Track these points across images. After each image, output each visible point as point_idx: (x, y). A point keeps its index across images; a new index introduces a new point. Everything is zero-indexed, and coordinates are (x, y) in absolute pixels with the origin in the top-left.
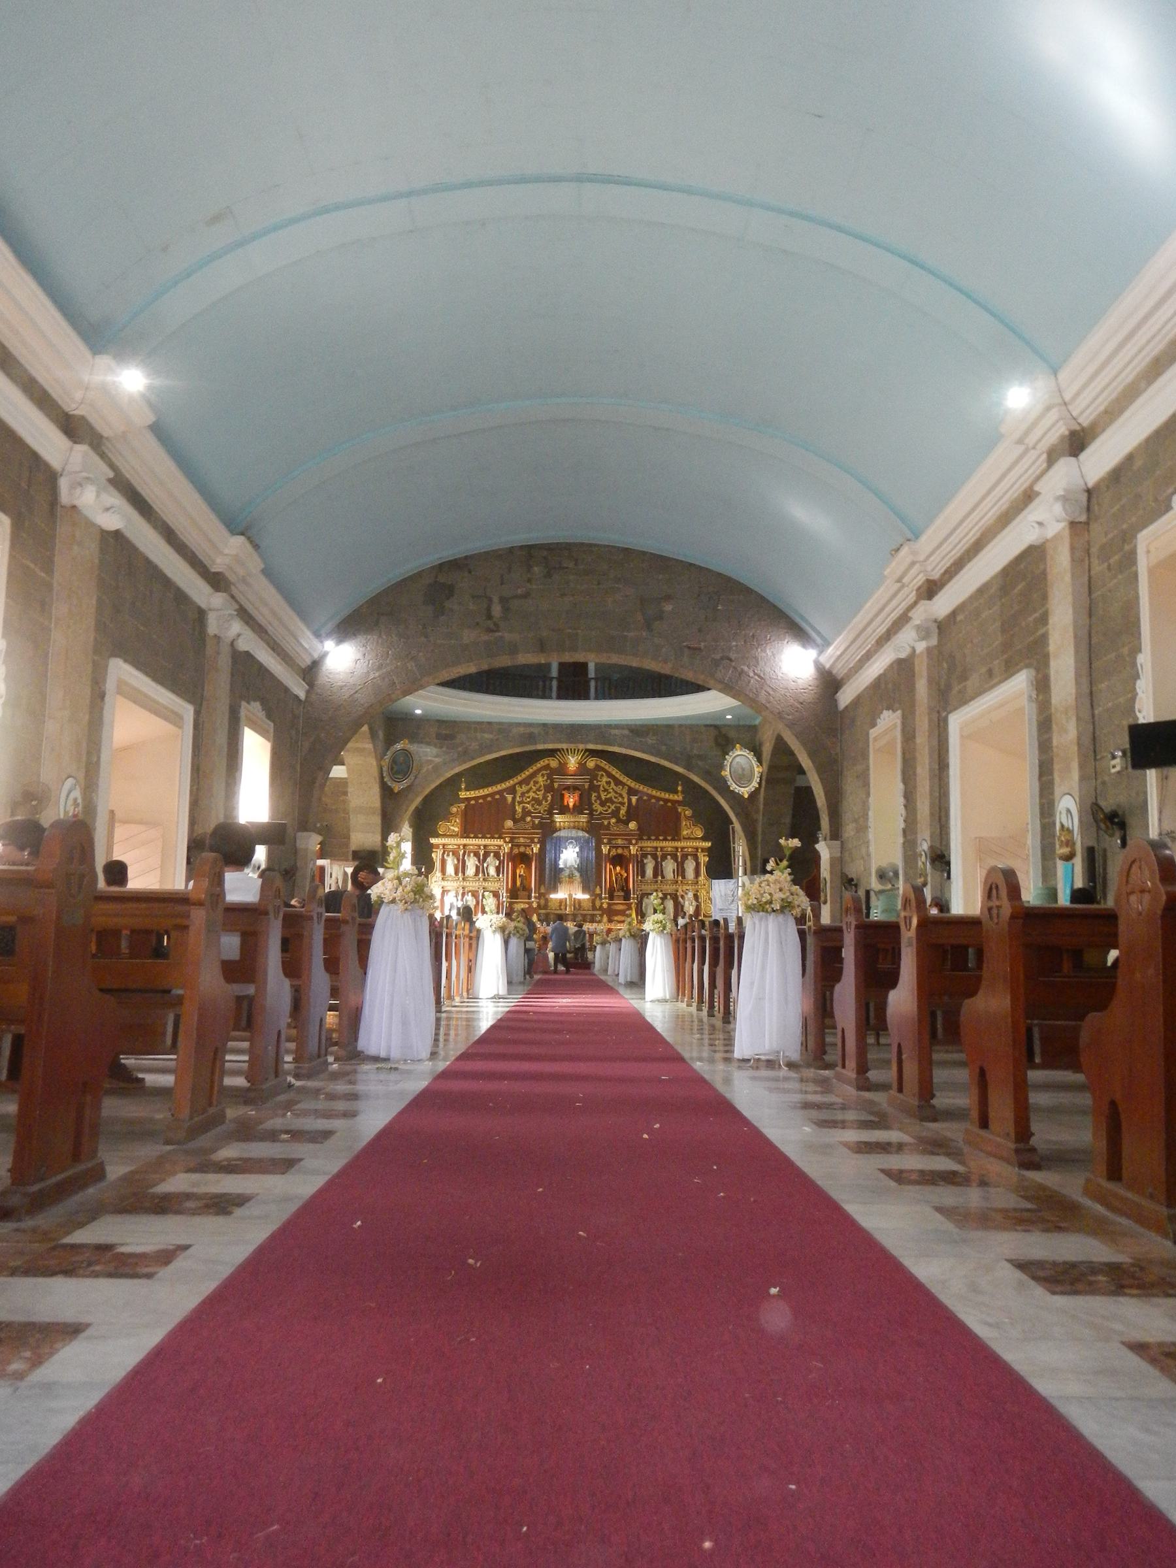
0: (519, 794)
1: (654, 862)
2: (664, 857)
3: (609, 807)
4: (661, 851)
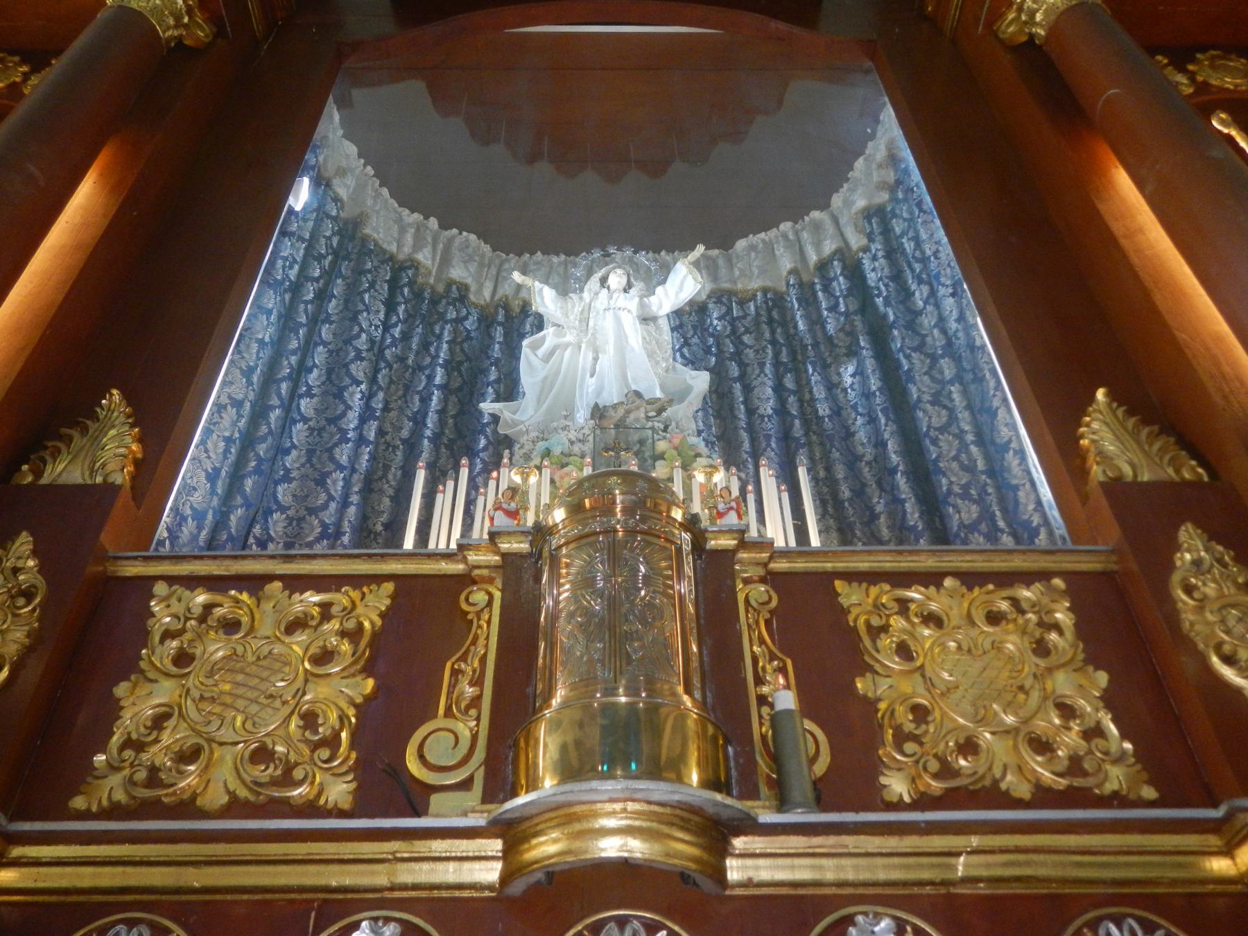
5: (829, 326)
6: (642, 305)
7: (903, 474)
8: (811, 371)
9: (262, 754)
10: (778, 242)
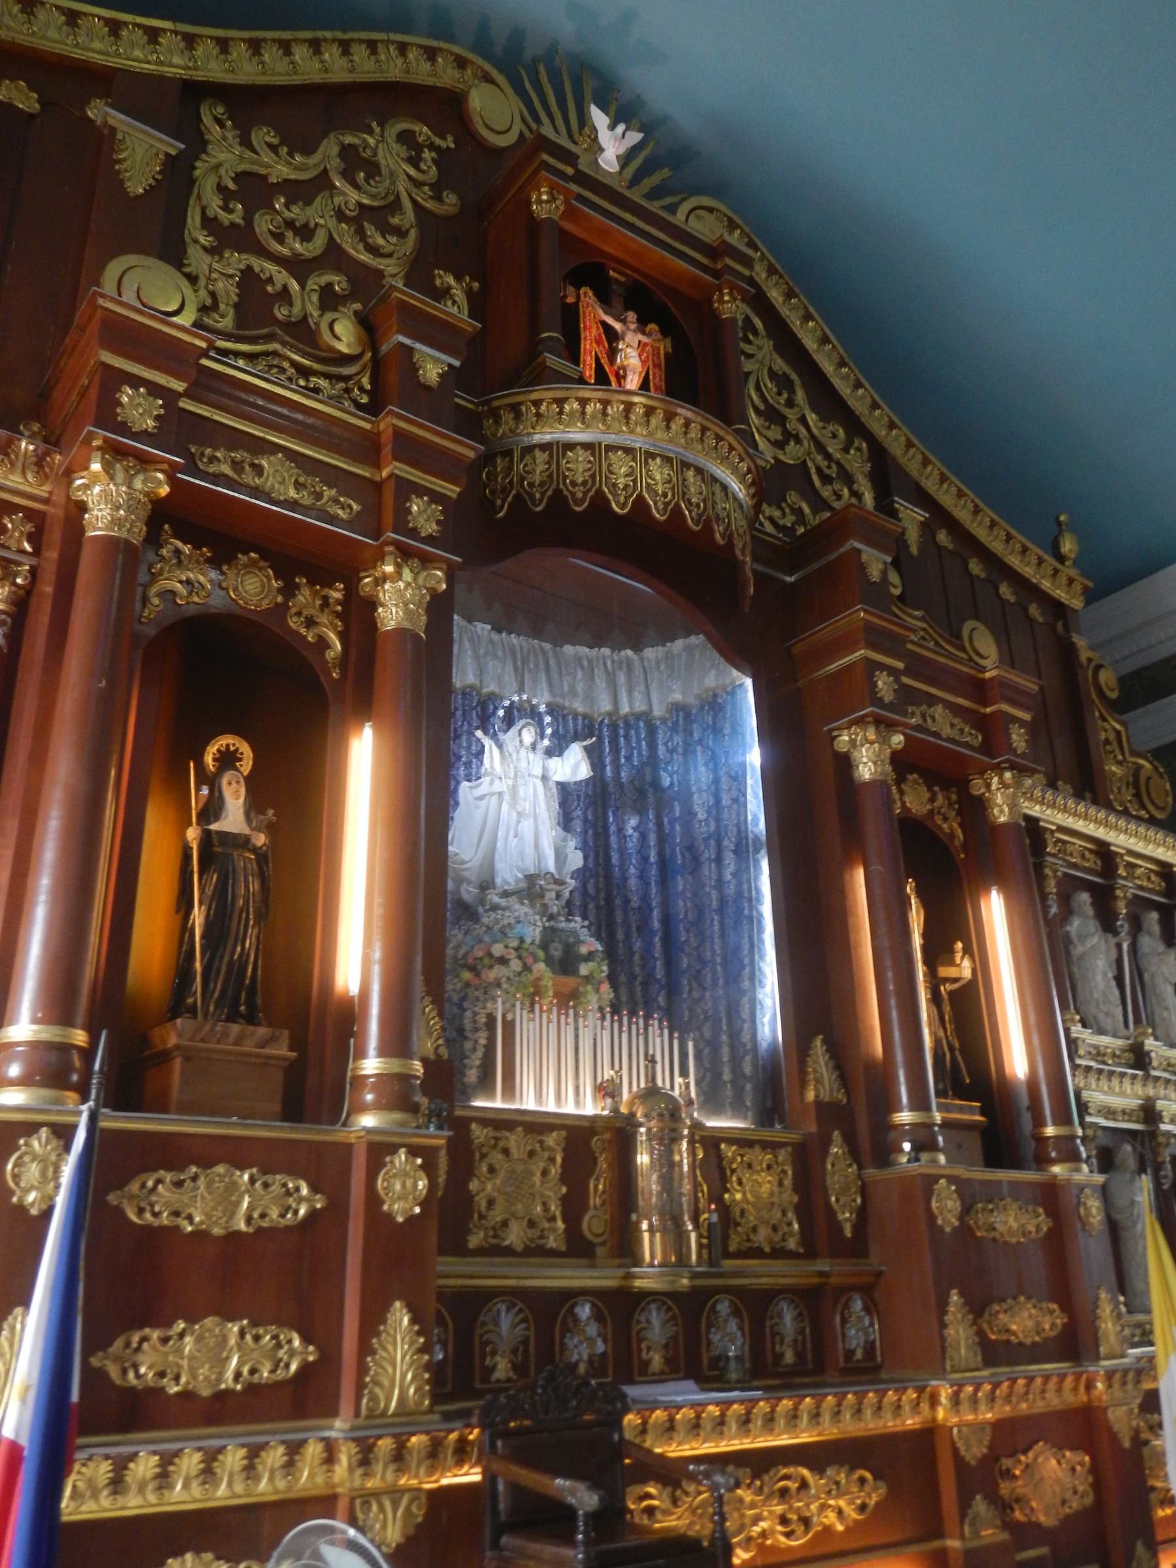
5: (623, 774)
6: (545, 768)
7: (661, 939)
8: (611, 819)
9: (531, 1224)
10: (598, 665)
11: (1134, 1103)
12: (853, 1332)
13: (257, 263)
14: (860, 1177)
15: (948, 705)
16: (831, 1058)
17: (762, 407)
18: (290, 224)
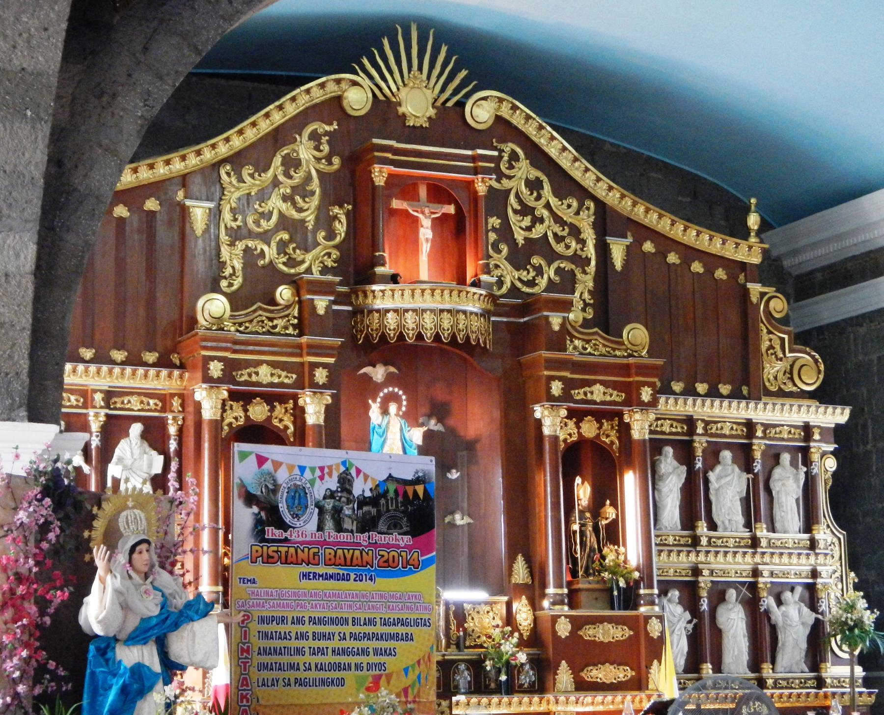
0: (233, 196)
1: (684, 468)
2: (713, 456)
3: (539, 271)
4: (706, 433)
11: (749, 567)
12: (523, 677)
13: (251, 244)
14: (534, 615)
15: (603, 383)
16: (526, 563)
17: (519, 208)
18: (262, 215)
